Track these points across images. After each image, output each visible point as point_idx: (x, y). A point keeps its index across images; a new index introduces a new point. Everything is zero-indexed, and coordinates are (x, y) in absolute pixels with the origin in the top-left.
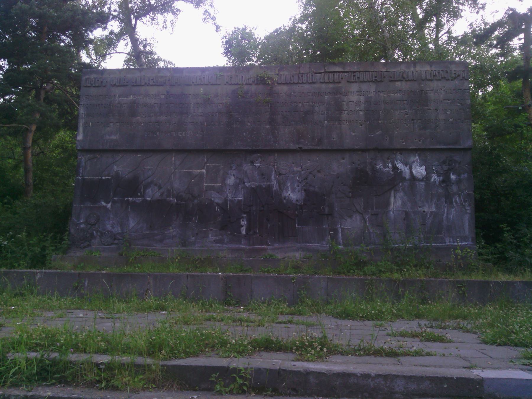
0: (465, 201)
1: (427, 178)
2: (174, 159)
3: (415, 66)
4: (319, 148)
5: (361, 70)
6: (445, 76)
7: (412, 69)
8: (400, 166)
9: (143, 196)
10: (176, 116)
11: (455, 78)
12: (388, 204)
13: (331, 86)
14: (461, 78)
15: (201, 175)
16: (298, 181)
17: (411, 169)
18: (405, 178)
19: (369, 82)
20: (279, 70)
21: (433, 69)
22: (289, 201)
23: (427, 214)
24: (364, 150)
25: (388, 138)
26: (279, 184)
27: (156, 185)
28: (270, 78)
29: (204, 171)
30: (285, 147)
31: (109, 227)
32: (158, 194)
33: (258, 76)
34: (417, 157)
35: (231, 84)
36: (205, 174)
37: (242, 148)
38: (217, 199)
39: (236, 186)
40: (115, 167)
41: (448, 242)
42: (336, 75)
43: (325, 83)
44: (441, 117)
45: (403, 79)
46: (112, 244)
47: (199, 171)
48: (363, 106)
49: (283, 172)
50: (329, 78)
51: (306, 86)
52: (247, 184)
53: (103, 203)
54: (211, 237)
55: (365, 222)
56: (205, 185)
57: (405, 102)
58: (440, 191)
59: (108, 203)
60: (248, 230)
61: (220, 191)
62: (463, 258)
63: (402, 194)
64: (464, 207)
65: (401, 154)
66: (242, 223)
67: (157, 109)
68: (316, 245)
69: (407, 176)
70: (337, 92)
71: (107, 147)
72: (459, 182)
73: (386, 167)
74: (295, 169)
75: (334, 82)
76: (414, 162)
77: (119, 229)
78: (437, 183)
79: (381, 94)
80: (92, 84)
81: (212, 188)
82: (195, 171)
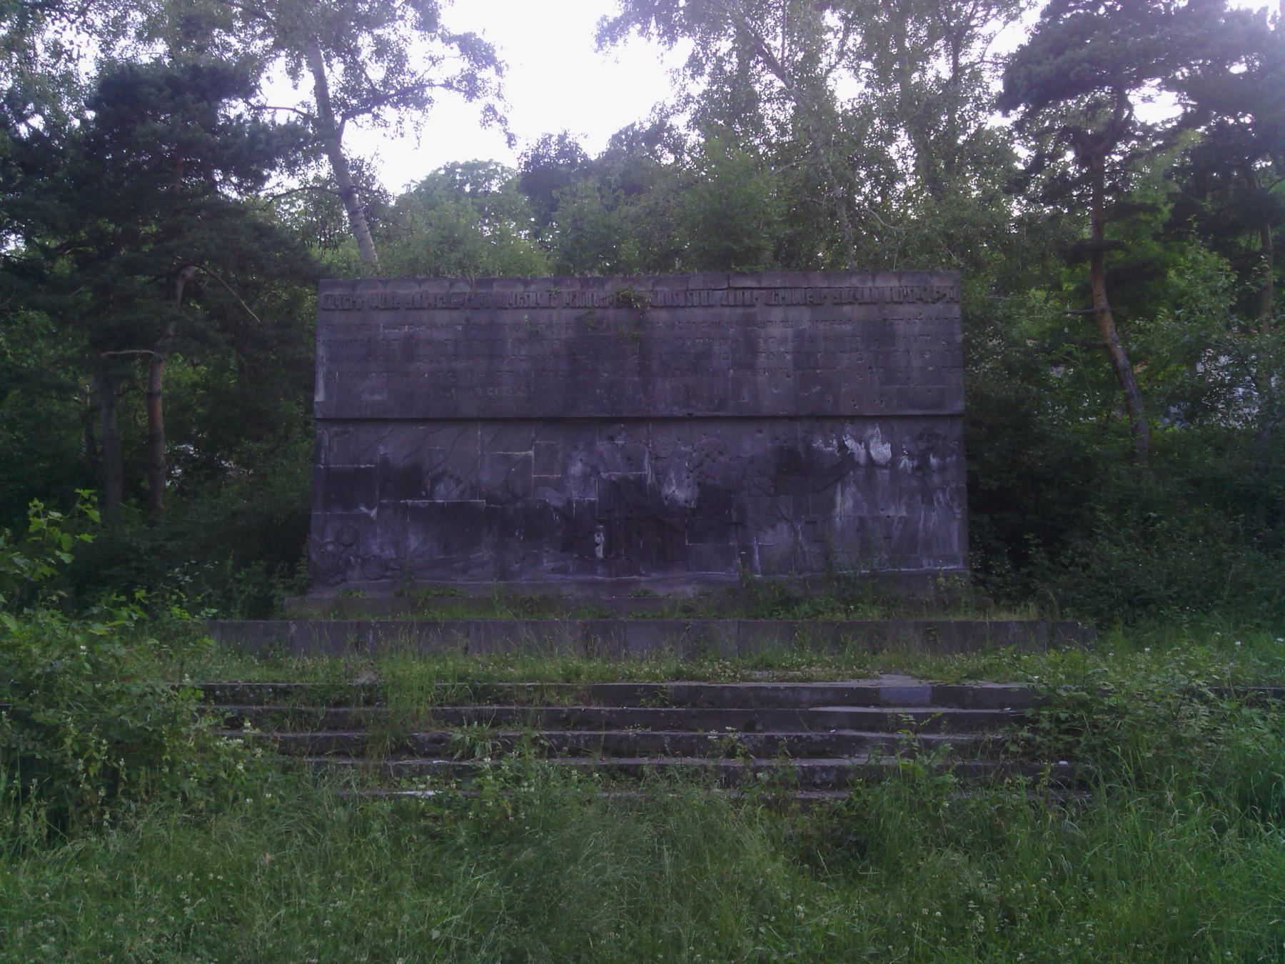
0: (952, 499)
1: (893, 462)
2: (480, 433)
3: (874, 279)
4: (717, 413)
5: (788, 285)
6: (923, 296)
7: (870, 284)
8: (850, 443)
9: (430, 495)
11: (938, 300)
12: (832, 505)
13: (739, 311)
14: (947, 299)
15: (527, 460)
17: (867, 448)
18: (858, 463)
19: (798, 304)
20: (654, 284)
21: (903, 283)
22: (674, 502)
23: (893, 521)
24: (793, 418)
25: (831, 398)
26: (657, 474)
27: (451, 477)
28: (639, 299)
29: (531, 453)
30: (666, 413)
31: (375, 549)
32: (455, 493)
33: (618, 293)
34: (878, 429)
35: (575, 307)
37: (594, 415)
38: (554, 499)
39: (585, 478)
40: (381, 448)
41: (927, 565)
42: (747, 293)
43: (730, 306)
44: (916, 363)
45: (855, 300)
46: (383, 577)
47: (523, 453)
48: (790, 345)
49: (662, 454)
50: (735, 298)
51: (699, 312)
52: (604, 475)
53: (364, 509)
54: (547, 564)
55: (796, 533)
57: (858, 339)
58: (914, 483)
59: (371, 508)
60: (607, 551)
61: (559, 486)
62: (948, 590)
63: (854, 489)
64: (951, 508)
65: (852, 423)
66: (597, 539)
68: (717, 574)
69: (862, 459)
70: (748, 321)
72: (943, 469)
73: (828, 445)
74: (683, 448)
75: (744, 305)
76: (872, 436)
77: (393, 551)
78: (910, 472)
79: (821, 326)
80: (337, 306)
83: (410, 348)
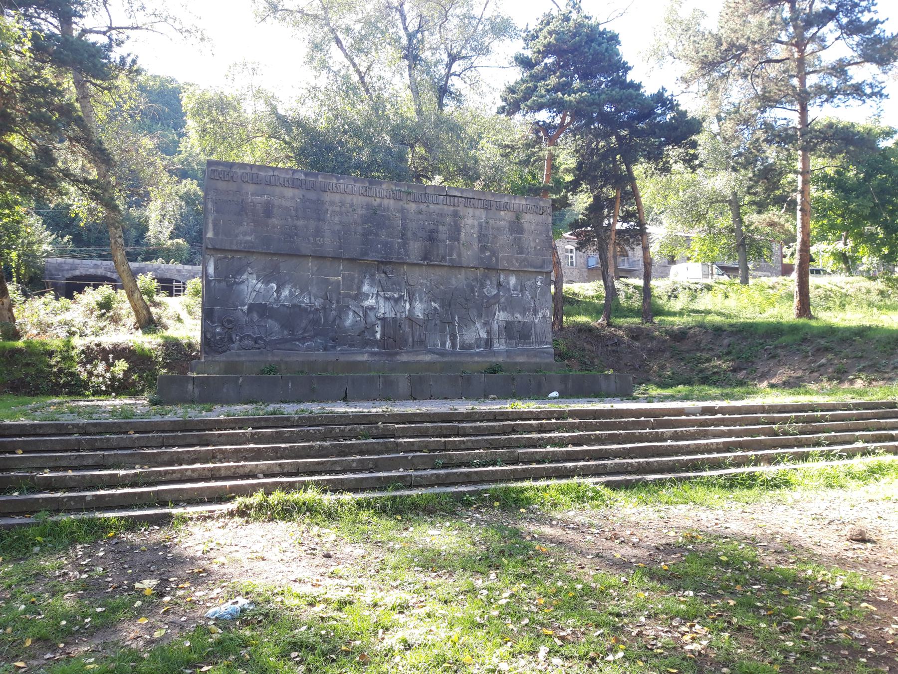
29: (340, 278)
42: (456, 199)
44: (533, 245)
48: (476, 229)
67: (293, 212)
70: (455, 214)
71: (241, 248)
75: (454, 205)
81: (348, 296)
83: (268, 210)
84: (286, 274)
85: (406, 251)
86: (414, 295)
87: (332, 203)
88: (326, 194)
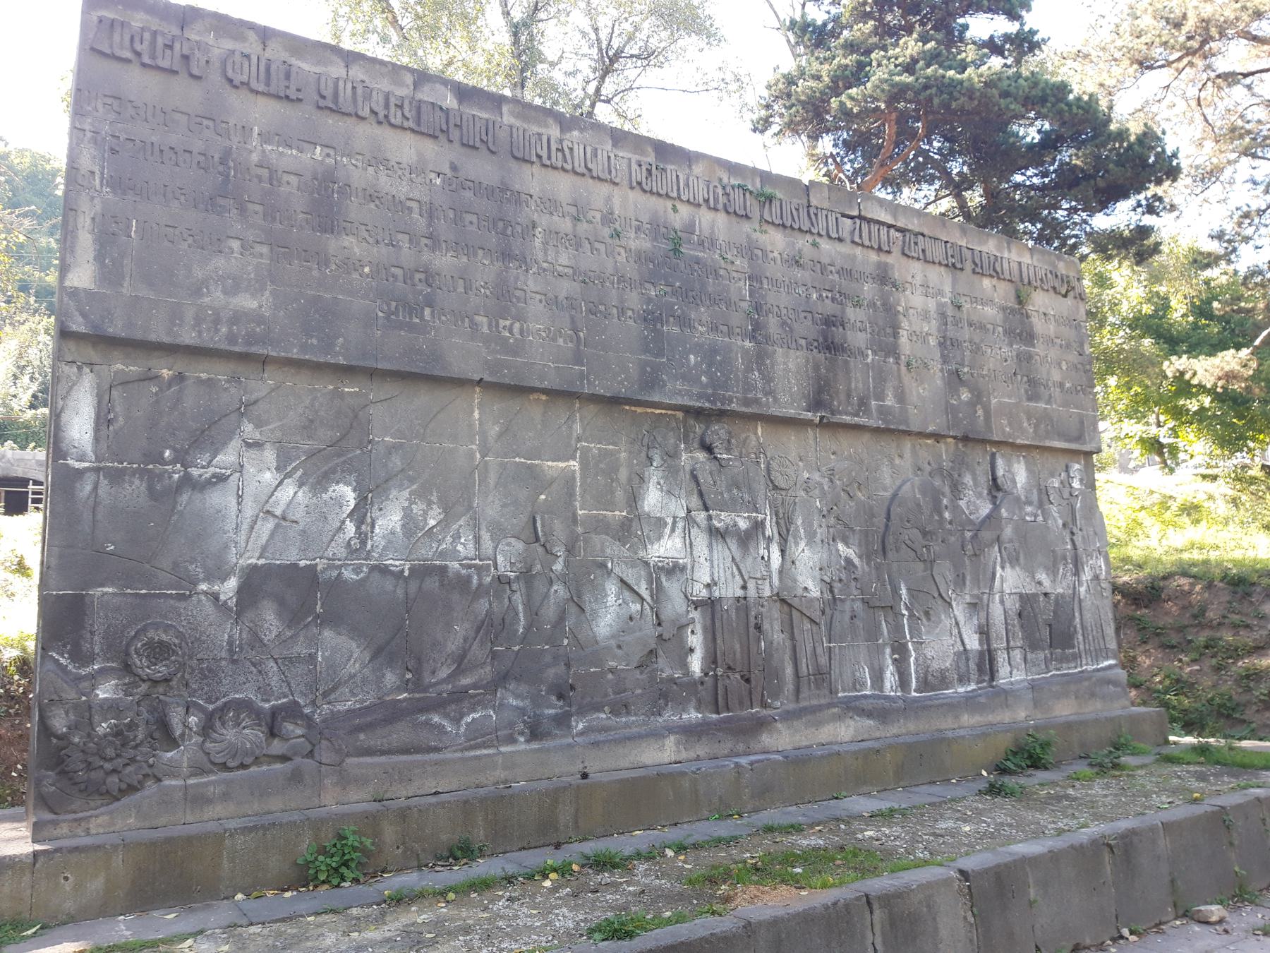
10: (486, 262)
16: (821, 511)
25: (980, 413)
29: (574, 465)
36: (578, 475)
49: (780, 481)
56: (580, 512)
70: (883, 277)
71: (217, 339)
80: (138, 54)
81: (601, 526)
82: (550, 463)
84: (392, 449)
85: (768, 379)
86: (790, 521)
87: (550, 204)
88: (526, 168)
